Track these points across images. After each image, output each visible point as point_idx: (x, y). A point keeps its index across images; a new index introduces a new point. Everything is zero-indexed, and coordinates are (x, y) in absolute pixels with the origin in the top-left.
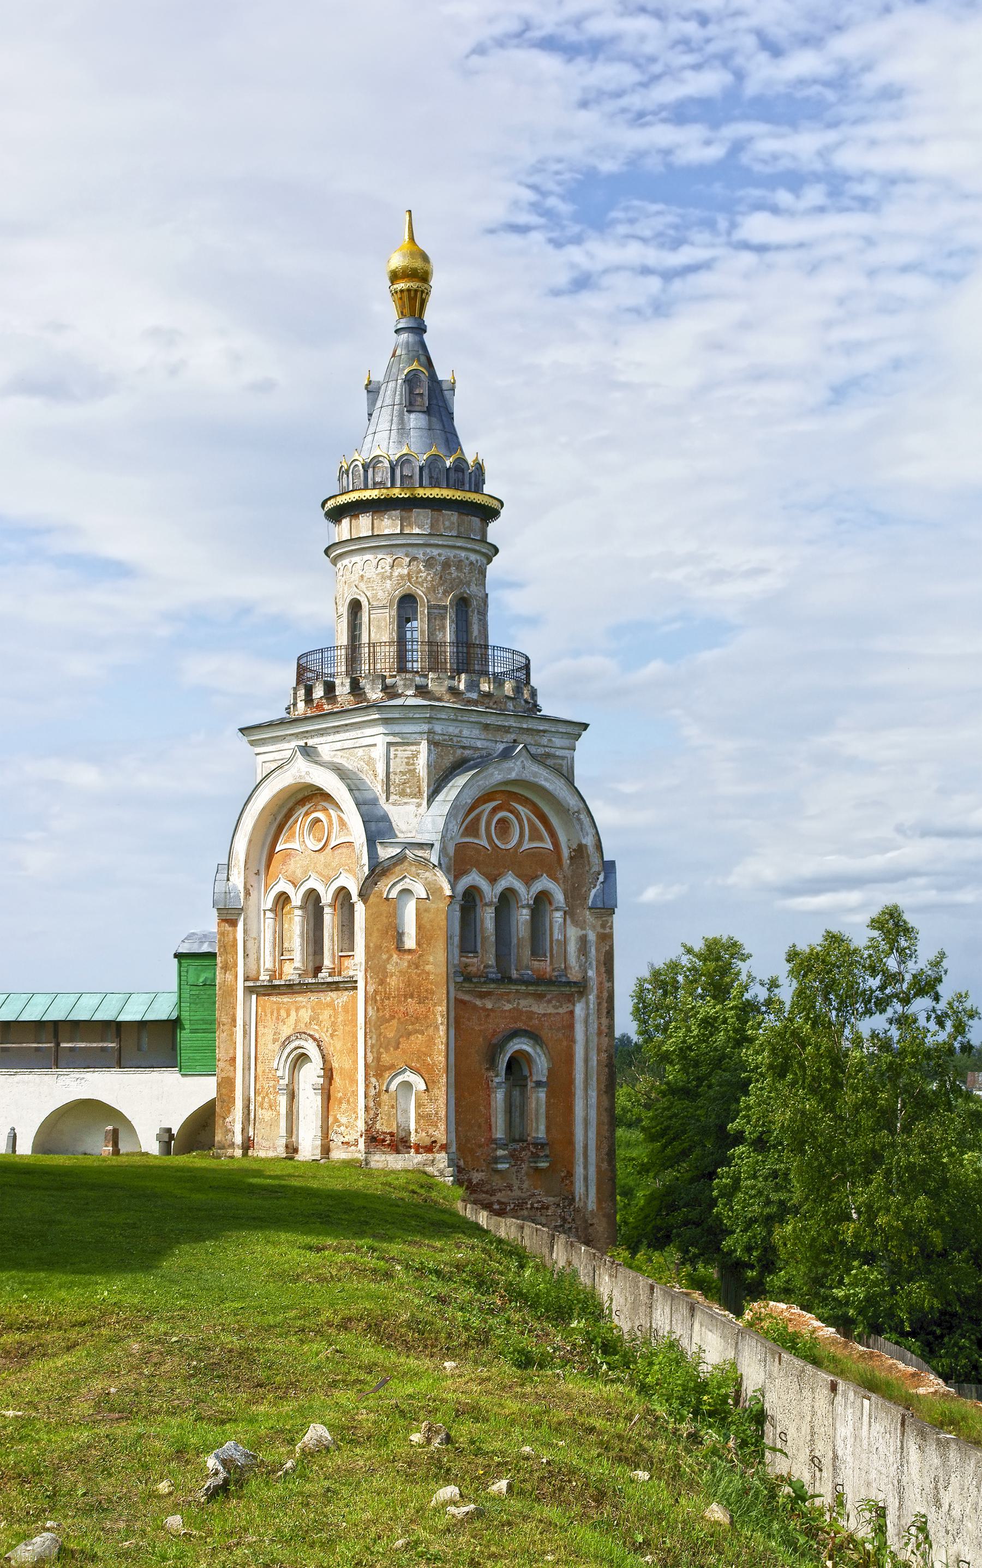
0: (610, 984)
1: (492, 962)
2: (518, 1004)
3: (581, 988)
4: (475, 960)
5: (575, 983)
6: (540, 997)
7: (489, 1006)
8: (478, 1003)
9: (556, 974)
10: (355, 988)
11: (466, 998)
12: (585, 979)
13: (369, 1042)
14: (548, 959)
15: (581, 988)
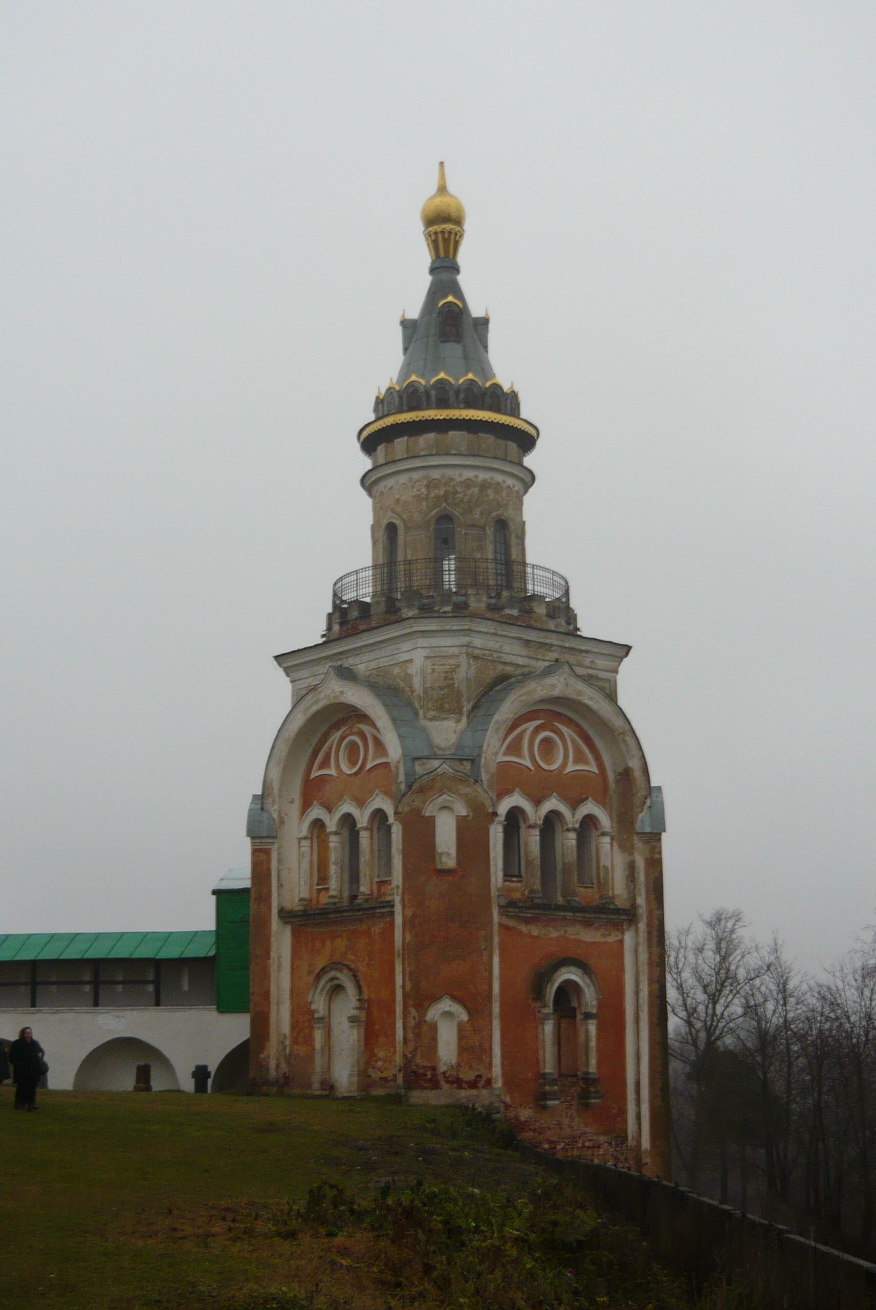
0: (659, 912)
1: (537, 886)
2: (566, 931)
3: (625, 916)
4: (519, 885)
5: (624, 910)
6: (588, 924)
7: (535, 932)
8: (524, 928)
9: (604, 901)
10: (392, 913)
11: (511, 923)
12: (634, 906)
13: (408, 969)
14: (595, 886)
15: (628, 916)
